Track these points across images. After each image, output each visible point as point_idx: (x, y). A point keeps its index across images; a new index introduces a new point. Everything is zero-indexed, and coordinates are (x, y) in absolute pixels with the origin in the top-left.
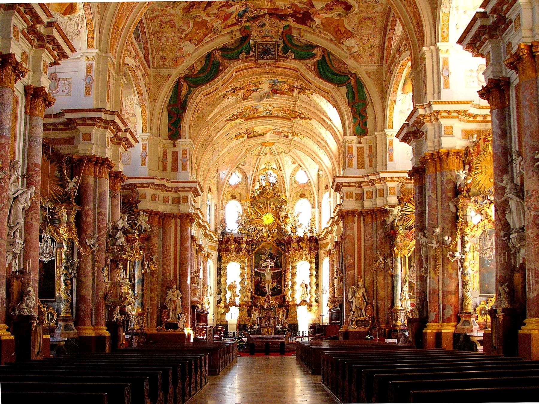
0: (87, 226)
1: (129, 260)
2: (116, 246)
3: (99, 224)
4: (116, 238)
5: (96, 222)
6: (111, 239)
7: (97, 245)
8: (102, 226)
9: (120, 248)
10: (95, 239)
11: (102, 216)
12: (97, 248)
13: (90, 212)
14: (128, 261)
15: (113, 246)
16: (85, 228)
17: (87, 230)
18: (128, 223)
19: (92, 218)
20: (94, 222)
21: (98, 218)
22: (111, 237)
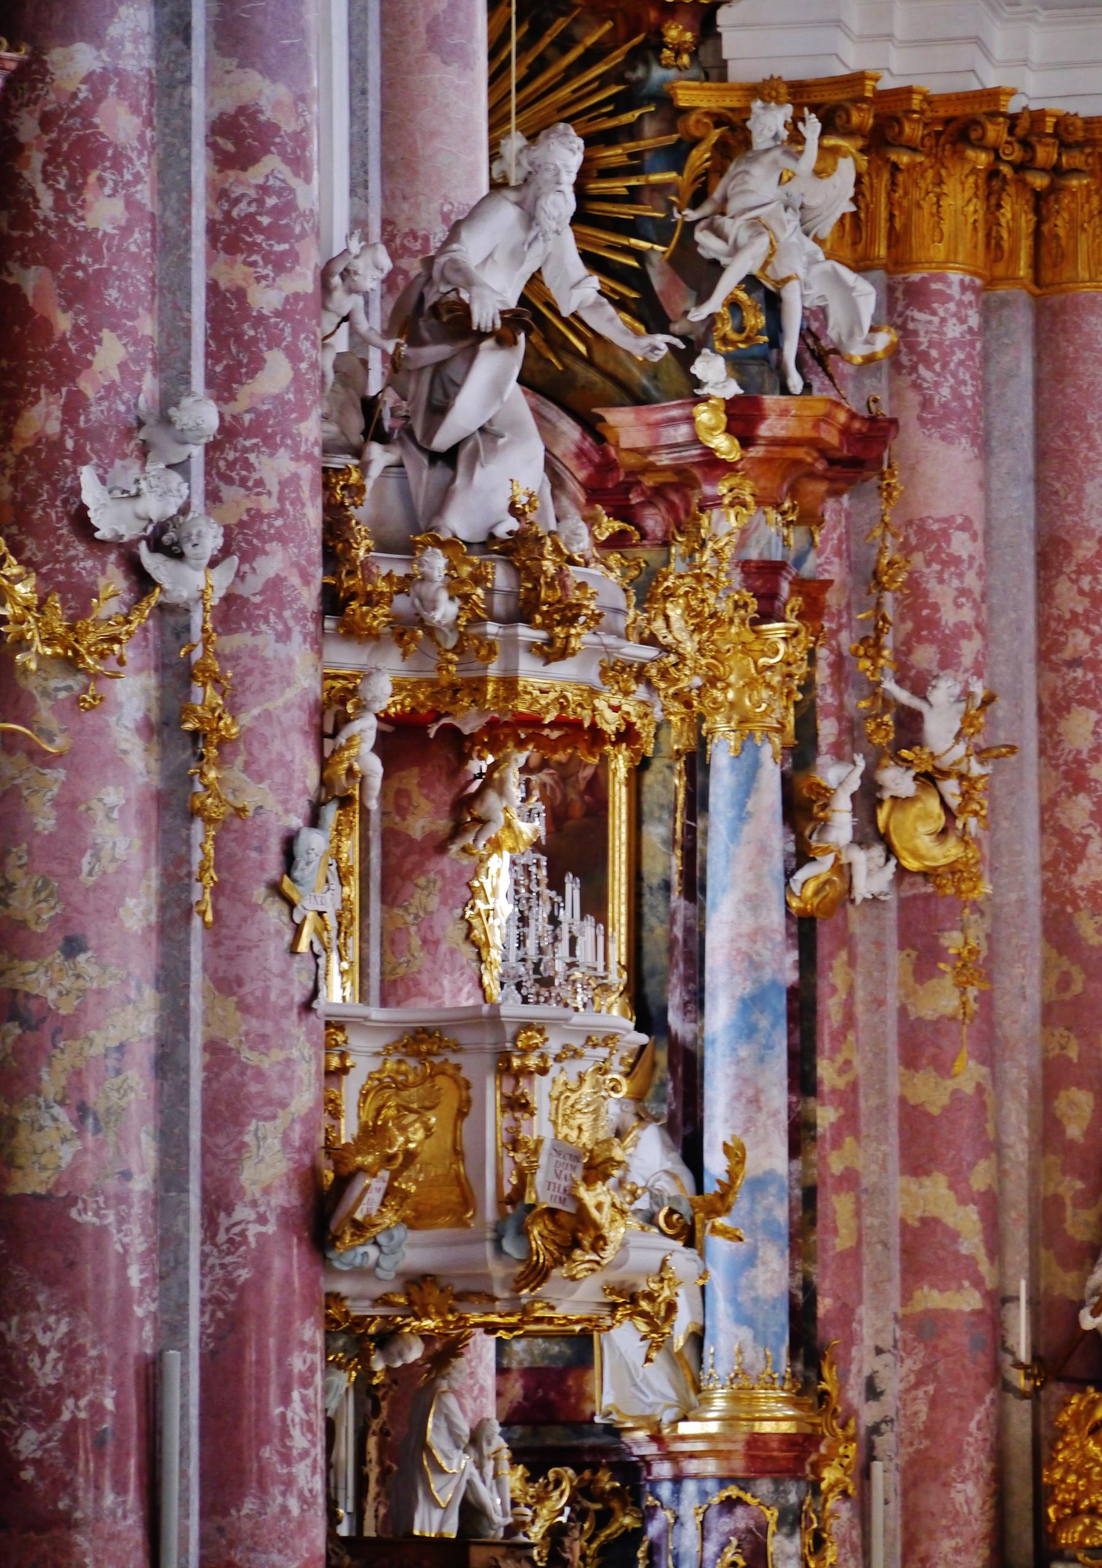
1: (610, 723)
2: (450, 545)
4: (442, 441)
5: (199, 242)
6: (379, 456)
7: (211, 539)
9: (501, 577)
10: (181, 468)
11: (270, 166)
12: (221, 580)
14: (596, 736)
15: (408, 549)
16: (64, 322)
17: (89, 344)
18: (587, 258)
19: (144, 193)
21: (219, 194)
22: (383, 438)
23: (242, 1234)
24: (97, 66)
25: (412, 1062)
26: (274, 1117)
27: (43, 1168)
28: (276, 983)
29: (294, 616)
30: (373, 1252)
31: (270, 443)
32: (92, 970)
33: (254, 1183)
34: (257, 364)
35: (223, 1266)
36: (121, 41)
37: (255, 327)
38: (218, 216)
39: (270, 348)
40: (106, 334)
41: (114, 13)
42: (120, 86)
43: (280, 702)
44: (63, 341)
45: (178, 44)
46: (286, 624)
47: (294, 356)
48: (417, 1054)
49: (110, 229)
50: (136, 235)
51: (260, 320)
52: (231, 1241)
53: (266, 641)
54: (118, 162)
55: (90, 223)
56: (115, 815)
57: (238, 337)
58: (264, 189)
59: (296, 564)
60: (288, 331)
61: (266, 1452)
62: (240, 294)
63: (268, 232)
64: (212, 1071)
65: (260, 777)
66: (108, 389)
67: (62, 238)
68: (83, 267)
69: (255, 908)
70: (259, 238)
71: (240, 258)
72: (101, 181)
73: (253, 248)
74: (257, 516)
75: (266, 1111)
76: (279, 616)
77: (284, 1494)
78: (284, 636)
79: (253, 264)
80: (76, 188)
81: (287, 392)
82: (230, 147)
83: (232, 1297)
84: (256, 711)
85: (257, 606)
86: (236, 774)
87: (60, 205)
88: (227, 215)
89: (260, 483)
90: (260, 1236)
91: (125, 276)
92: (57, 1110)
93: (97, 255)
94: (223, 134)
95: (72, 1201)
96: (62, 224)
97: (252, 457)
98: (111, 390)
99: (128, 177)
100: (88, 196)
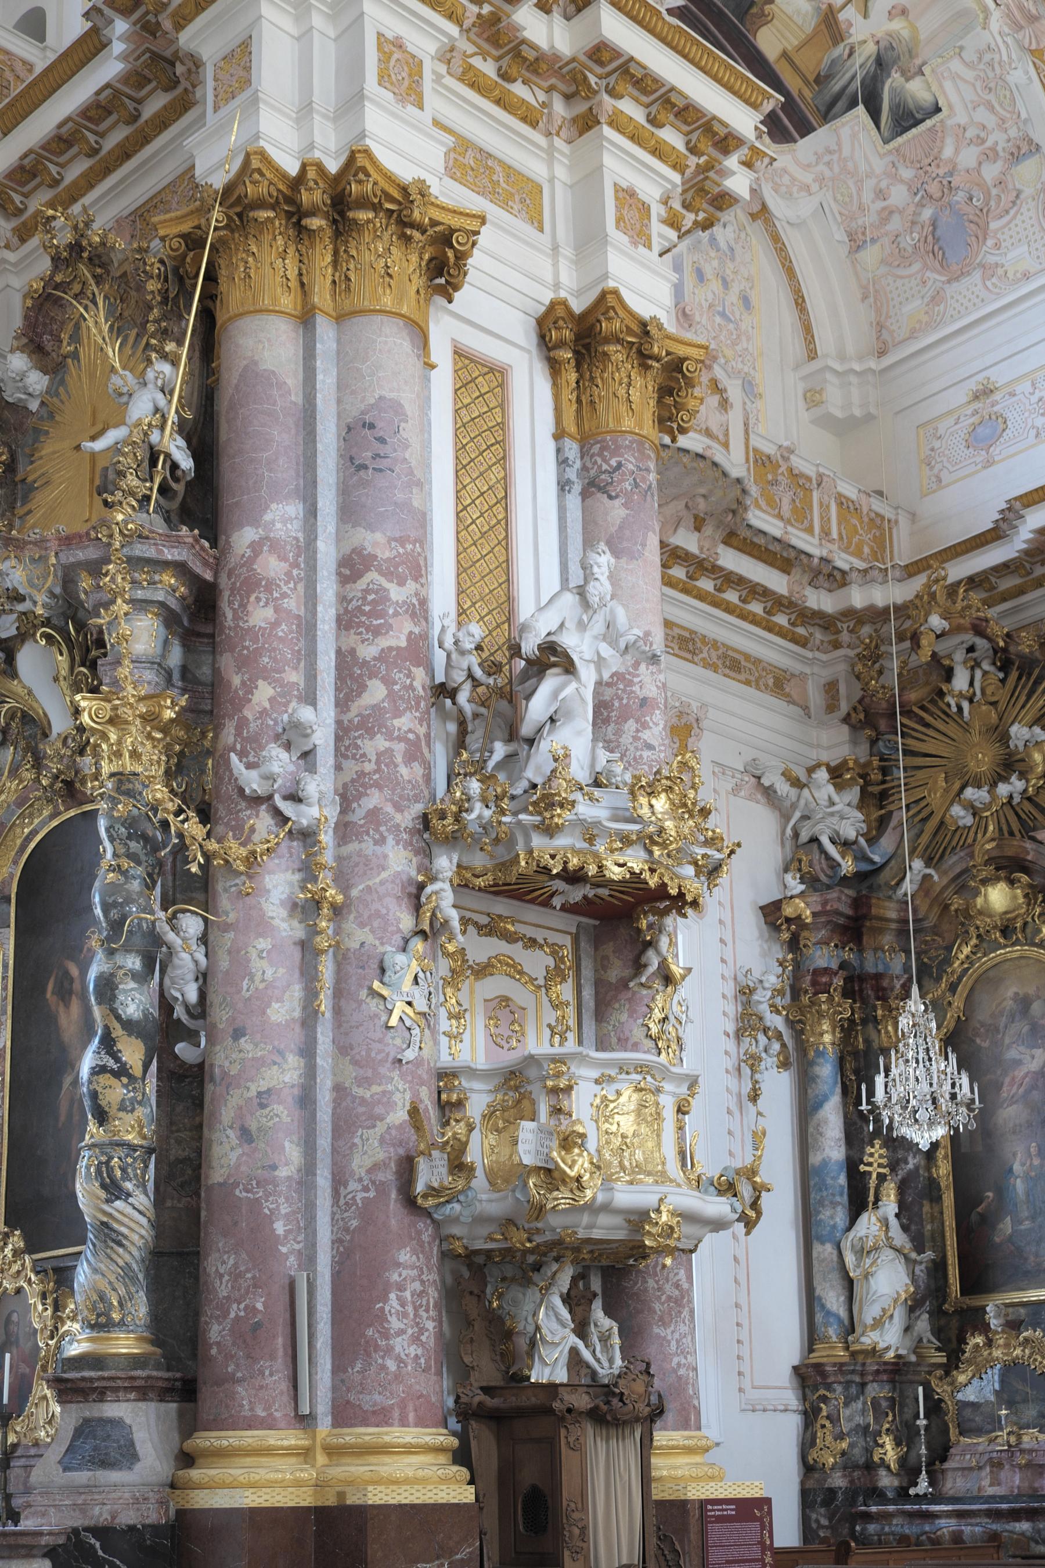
0: (244, 663)
3: (351, 640)
8: (368, 652)
13: (271, 566)
16: (236, 680)
17: (249, 688)
20: (308, 628)
21: (342, 599)
23: (353, 1198)
24: (256, 538)
25: (511, 1094)
26: (374, 1126)
27: (222, 1167)
28: (376, 1046)
29: (388, 830)
30: (457, 1206)
31: (371, 733)
32: (249, 1047)
33: (360, 1167)
34: (362, 688)
35: (343, 1219)
36: (273, 522)
37: (361, 668)
38: (342, 611)
39: (370, 678)
40: (260, 683)
41: (267, 507)
42: (271, 546)
43: (377, 880)
44: (236, 691)
45: (312, 520)
46: (381, 835)
47: (388, 682)
48: (510, 1088)
49: (263, 625)
50: (284, 627)
51: (365, 663)
52: (347, 1203)
53: (368, 846)
54: (268, 589)
55: (251, 623)
56: (264, 955)
57: (351, 676)
58: (367, 591)
59: (391, 800)
60: (383, 667)
61: (370, 1332)
62: (353, 652)
63: (369, 615)
64: (337, 1103)
65: (362, 925)
66: (261, 713)
67: (236, 634)
68: (247, 648)
69: (360, 1003)
70: (363, 619)
71: (352, 631)
72: (258, 599)
73: (360, 624)
74: (362, 774)
75: (368, 1123)
76: (377, 830)
77: (383, 1358)
78: (381, 841)
79: (361, 633)
80: (243, 606)
81: (383, 701)
82: (348, 572)
83: (348, 1238)
84: (361, 887)
85: (362, 826)
86: (350, 924)
87: (236, 618)
88: (346, 609)
89: (364, 755)
90: (364, 1199)
91: (274, 650)
92: (229, 1132)
93: (255, 640)
94: (344, 566)
95: (236, 1184)
96: (238, 626)
97: (359, 742)
98: (264, 713)
99: (276, 595)
100: (250, 608)
